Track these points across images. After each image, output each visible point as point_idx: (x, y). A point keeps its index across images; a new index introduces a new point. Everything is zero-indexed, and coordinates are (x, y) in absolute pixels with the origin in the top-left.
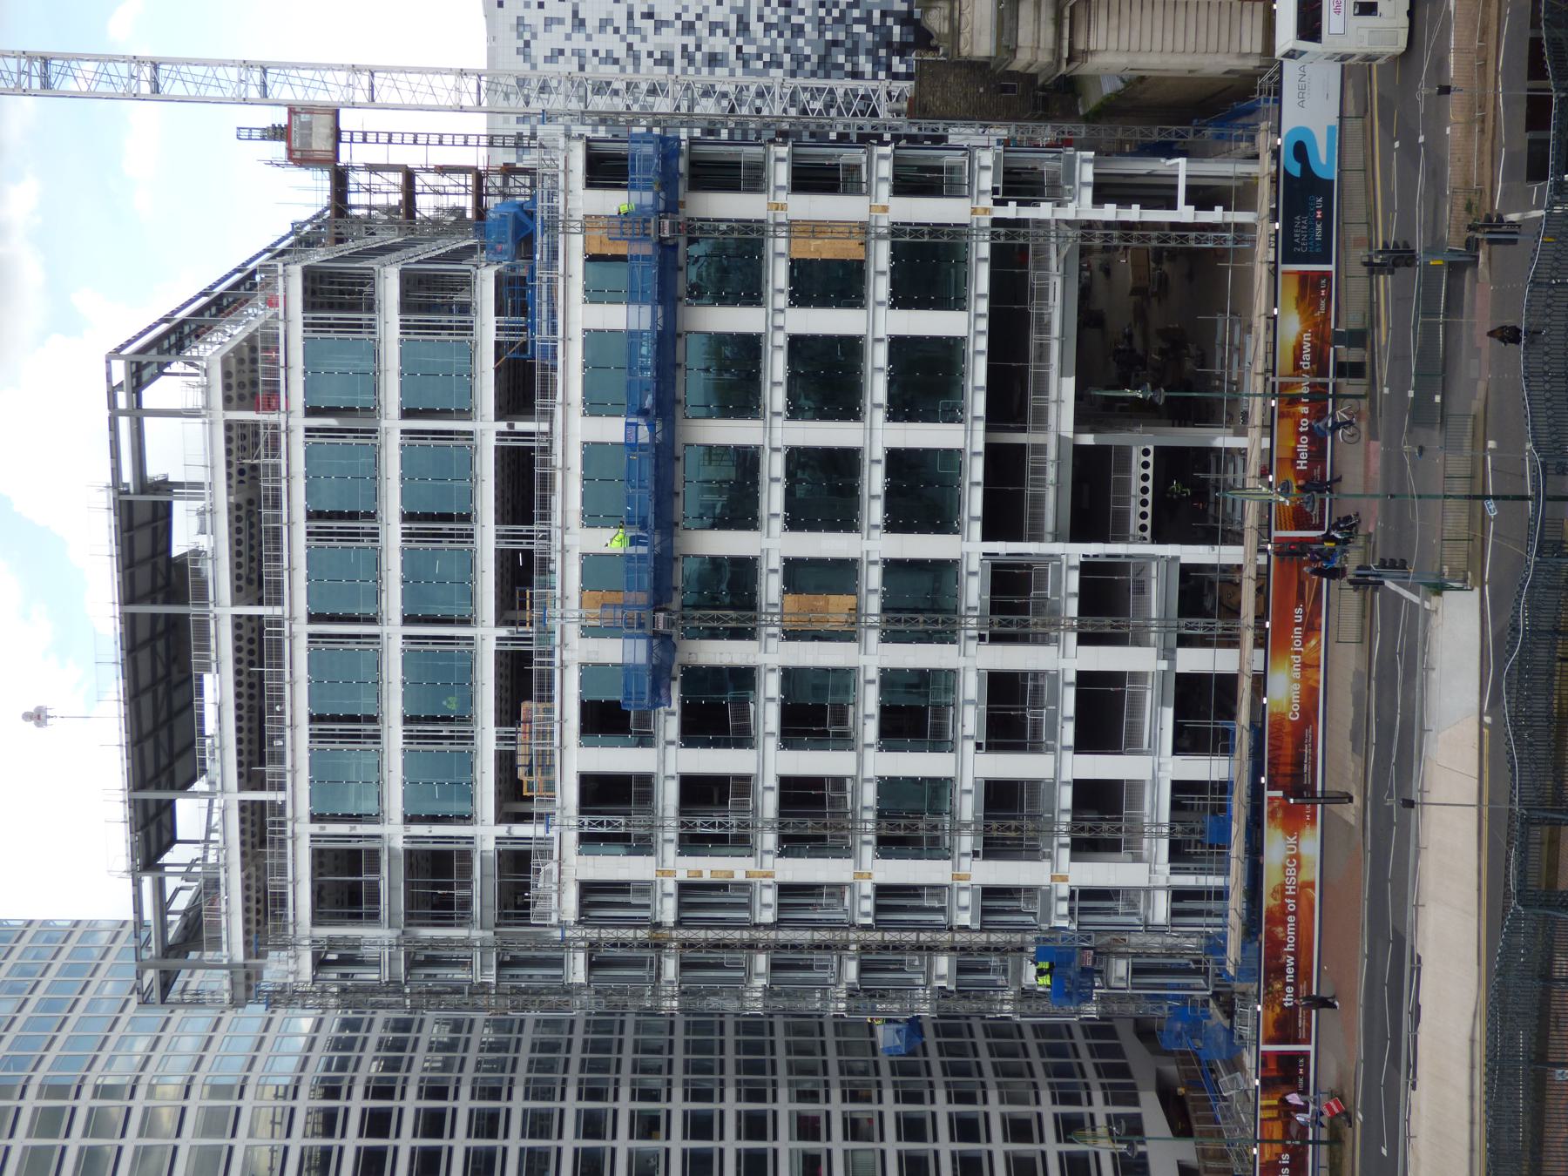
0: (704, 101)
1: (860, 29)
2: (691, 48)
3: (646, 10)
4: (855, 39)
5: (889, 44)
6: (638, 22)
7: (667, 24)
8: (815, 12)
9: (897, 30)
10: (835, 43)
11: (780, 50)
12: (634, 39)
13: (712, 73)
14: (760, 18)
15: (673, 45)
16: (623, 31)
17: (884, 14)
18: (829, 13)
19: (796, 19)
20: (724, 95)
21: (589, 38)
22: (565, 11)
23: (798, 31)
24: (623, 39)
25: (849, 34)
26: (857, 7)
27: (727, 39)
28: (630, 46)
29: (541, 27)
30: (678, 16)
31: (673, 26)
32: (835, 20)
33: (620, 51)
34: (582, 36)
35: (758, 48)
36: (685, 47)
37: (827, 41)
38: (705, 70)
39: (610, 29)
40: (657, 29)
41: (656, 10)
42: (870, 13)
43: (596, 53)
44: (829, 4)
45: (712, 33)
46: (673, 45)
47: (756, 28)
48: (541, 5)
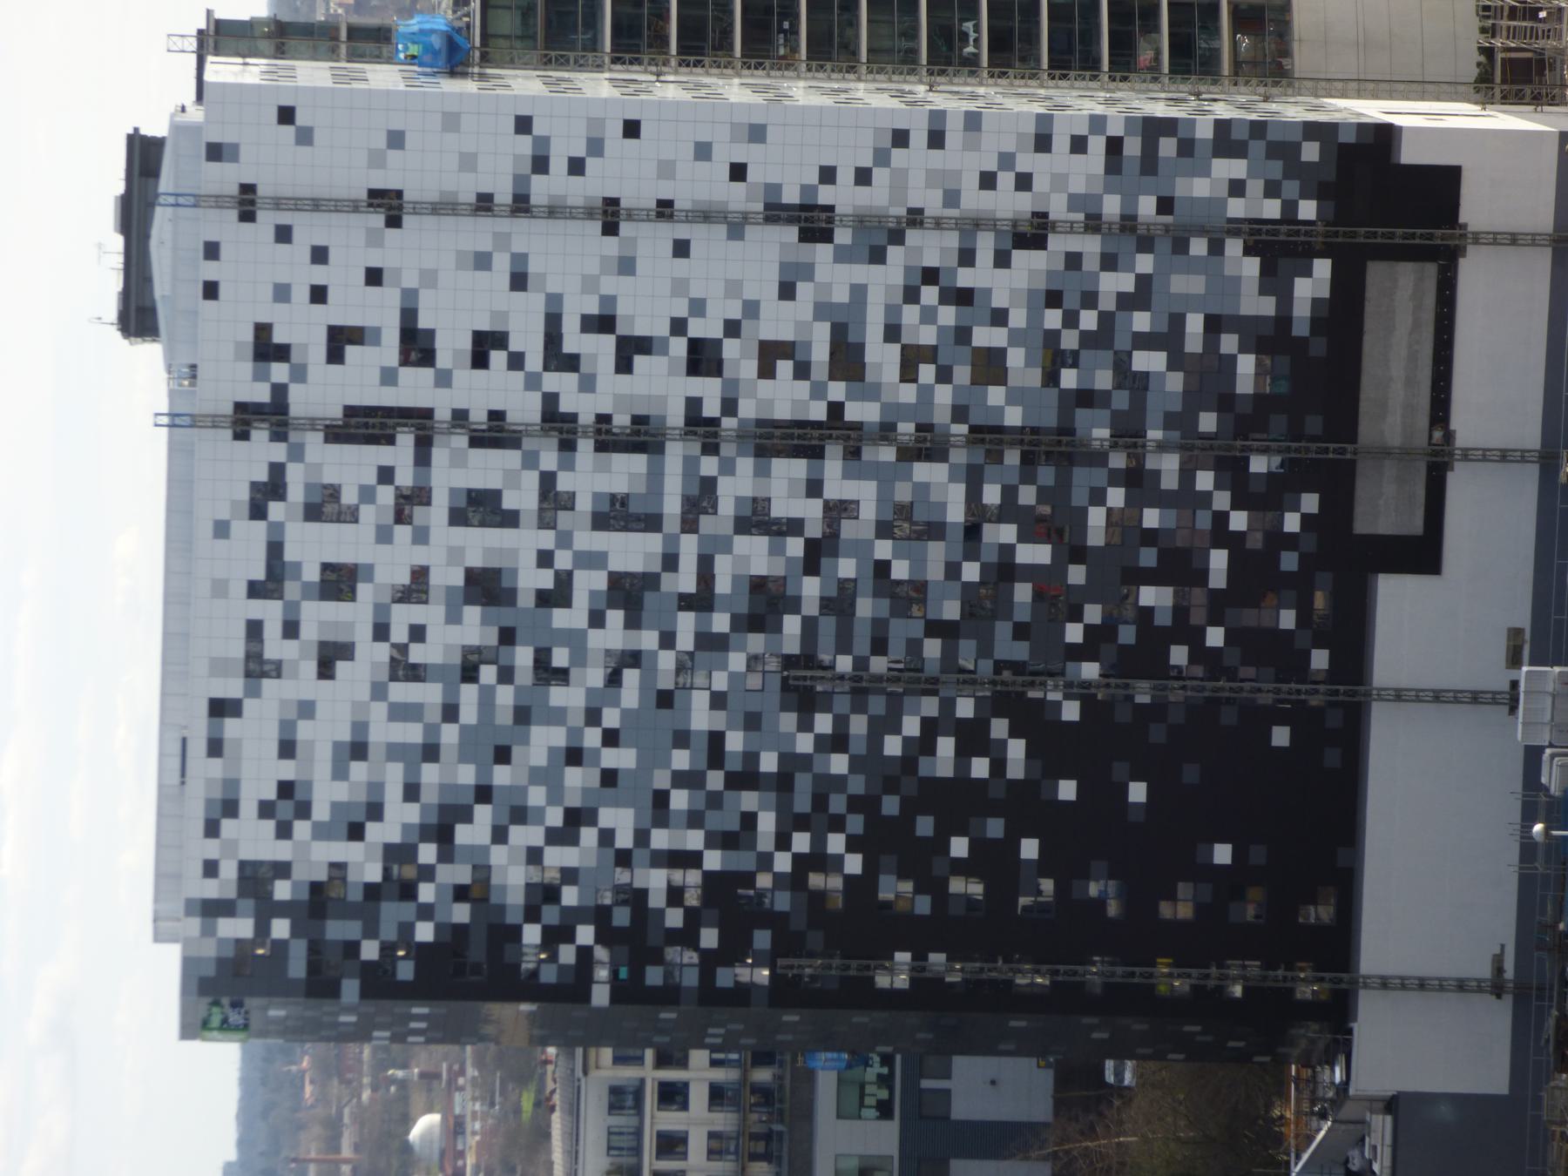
0: (742, 543)
1: (1149, 361)
2: (711, 409)
3: (593, 308)
4: (1139, 384)
5: (1226, 402)
6: (574, 340)
7: (644, 345)
8: (1035, 317)
9: (1246, 365)
10: (1086, 397)
11: (941, 416)
12: (562, 383)
13: (762, 472)
14: (892, 332)
15: (663, 400)
16: (534, 361)
17: (1214, 325)
18: (1071, 320)
19: (985, 337)
20: (794, 526)
21: (444, 379)
22: (382, 312)
23: (990, 366)
24: (532, 382)
25: (1125, 376)
26: (1145, 306)
27: (803, 387)
28: (551, 400)
29: (319, 350)
30: (678, 326)
31: (664, 351)
32: (1087, 339)
33: (524, 409)
34: (426, 374)
35: (886, 408)
36: (693, 404)
37: (1065, 393)
38: (745, 465)
39: (498, 358)
40: (624, 365)
41: (621, 310)
42: (1177, 322)
43: (460, 416)
44: (1072, 301)
45: (767, 371)
46: (663, 400)
47: (882, 358)
48: (319, 295)
